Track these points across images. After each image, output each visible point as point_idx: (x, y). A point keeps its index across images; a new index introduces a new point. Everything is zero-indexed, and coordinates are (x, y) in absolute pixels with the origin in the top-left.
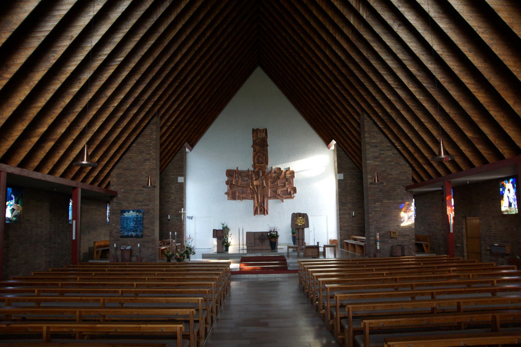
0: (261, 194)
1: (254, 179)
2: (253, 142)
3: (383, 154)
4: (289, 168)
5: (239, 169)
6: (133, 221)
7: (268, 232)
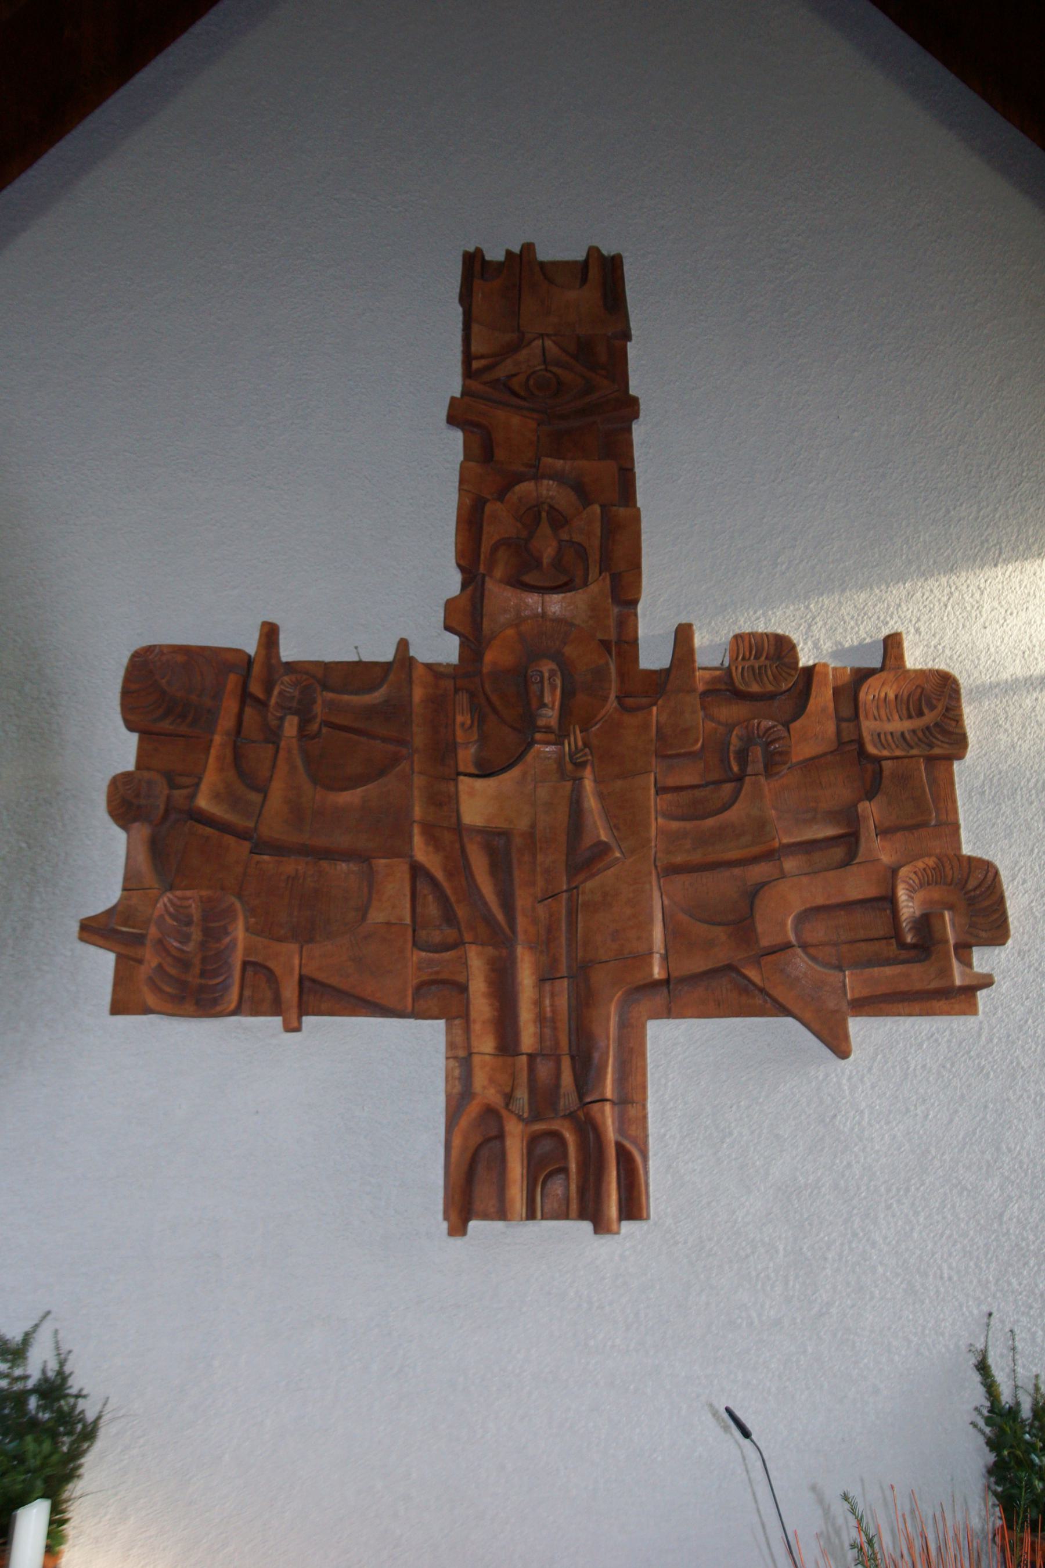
0: (544, 945)
1: (466, 756)
2: (468, 373)
4: (892, 644)
5: (289, 651)
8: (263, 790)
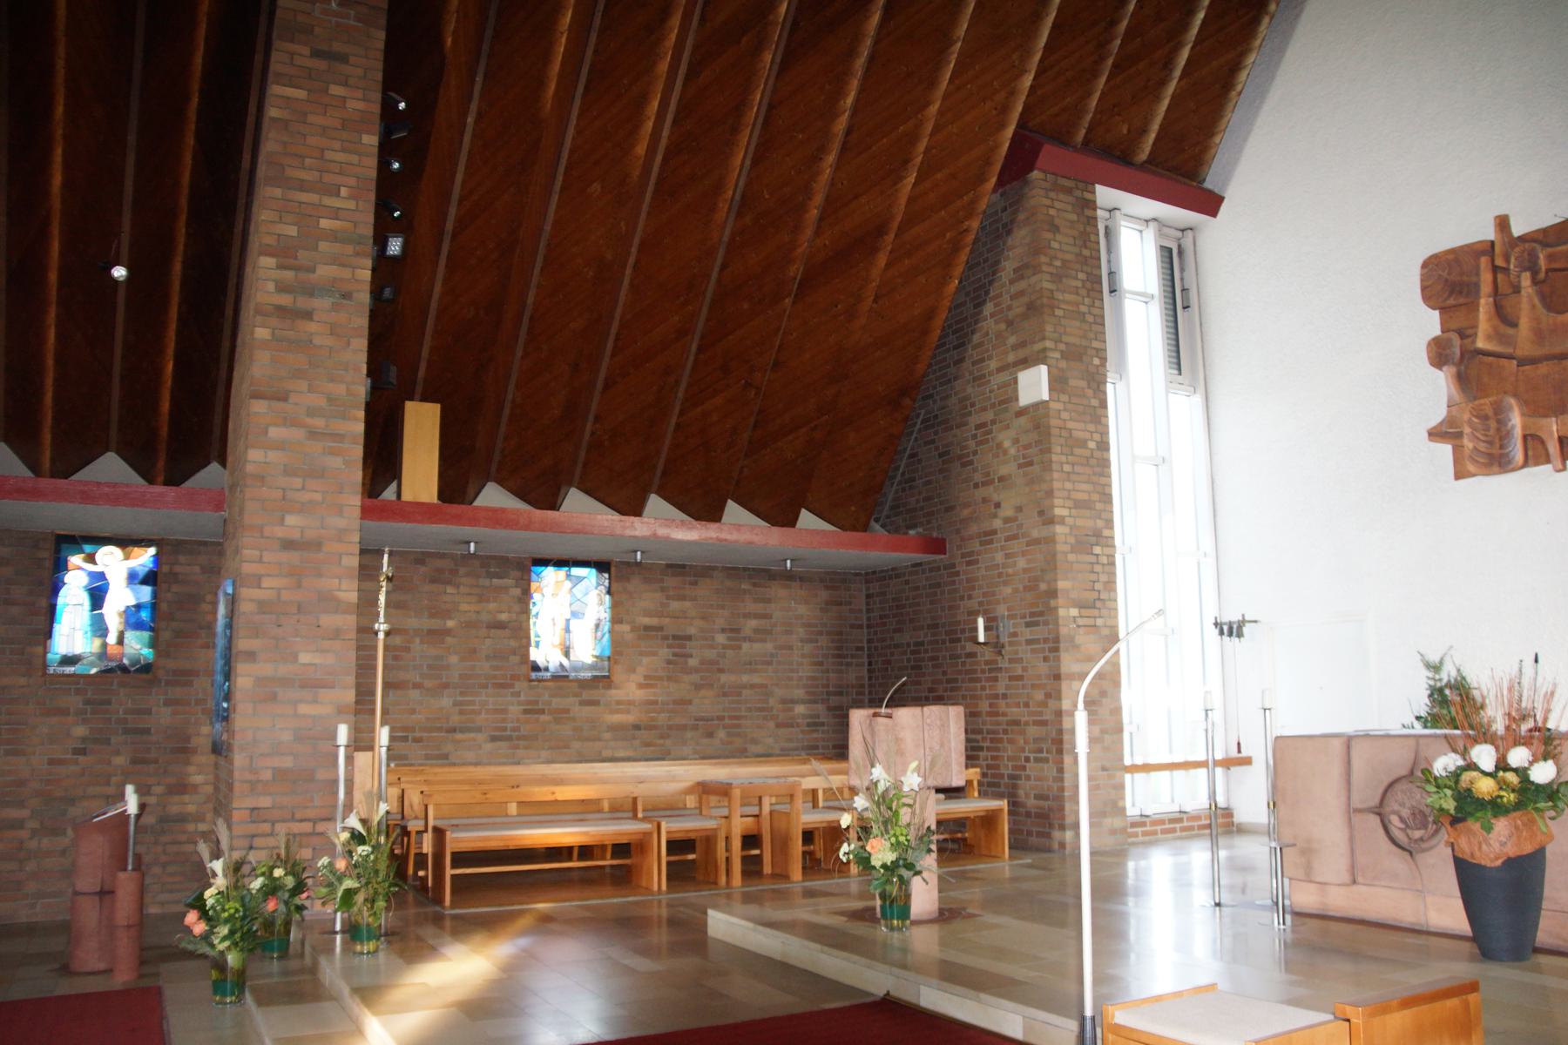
8: (1514, 325)
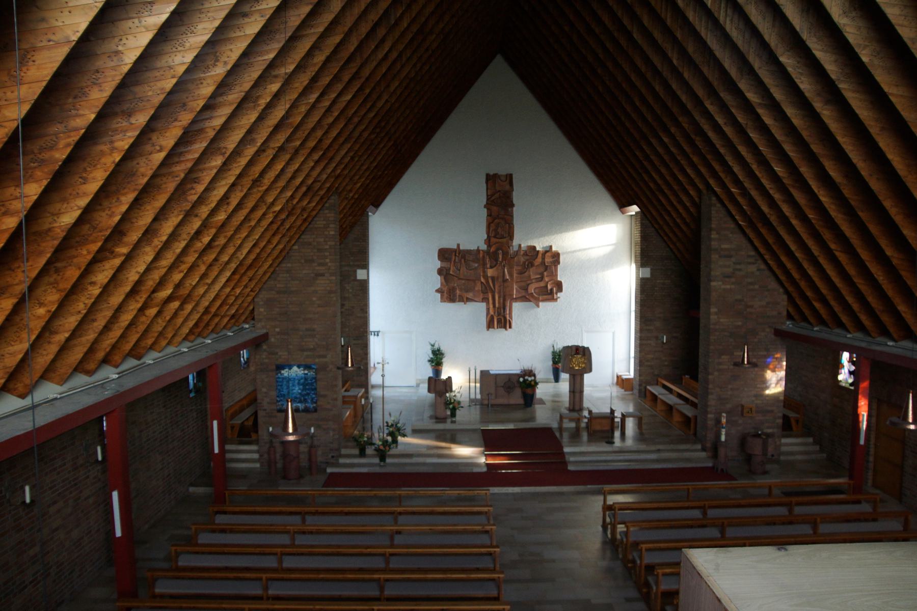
0: (499, 293)
1: (488, 266)
2: (488, 199)
3: (740, 270)
4: (551, 247)
5: (461, 248)
6: (299, 384)
7: (519, 376)
